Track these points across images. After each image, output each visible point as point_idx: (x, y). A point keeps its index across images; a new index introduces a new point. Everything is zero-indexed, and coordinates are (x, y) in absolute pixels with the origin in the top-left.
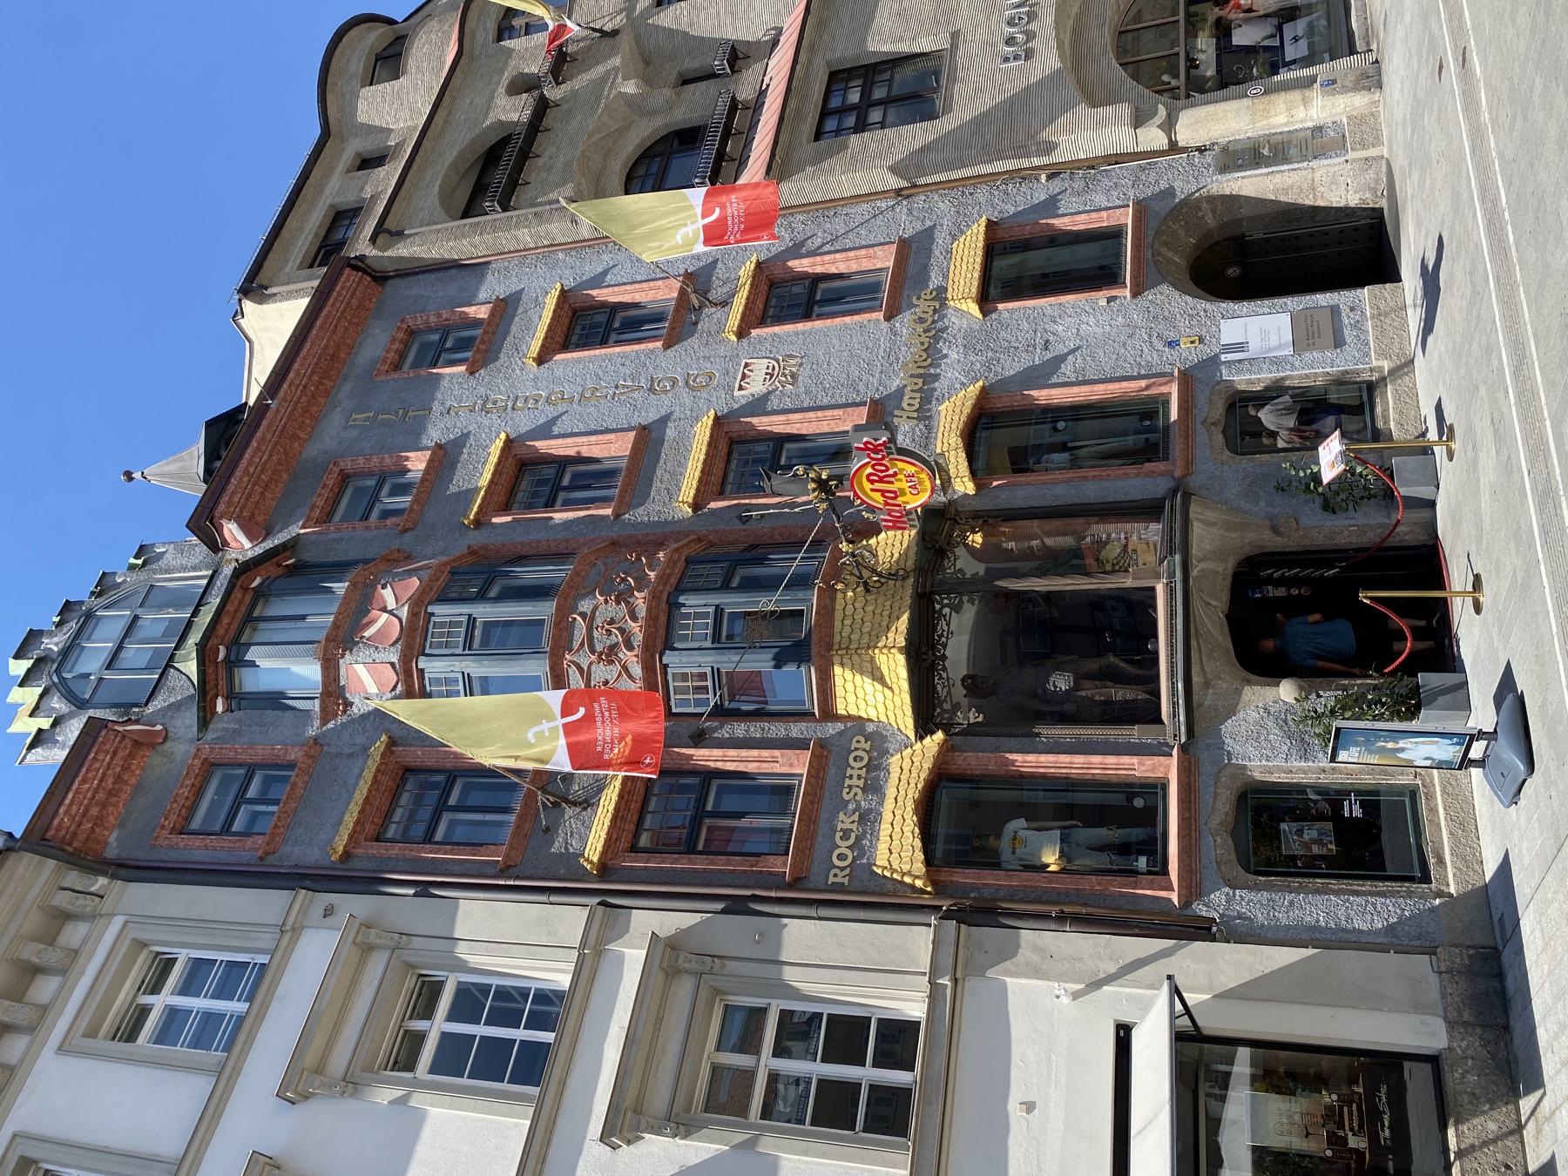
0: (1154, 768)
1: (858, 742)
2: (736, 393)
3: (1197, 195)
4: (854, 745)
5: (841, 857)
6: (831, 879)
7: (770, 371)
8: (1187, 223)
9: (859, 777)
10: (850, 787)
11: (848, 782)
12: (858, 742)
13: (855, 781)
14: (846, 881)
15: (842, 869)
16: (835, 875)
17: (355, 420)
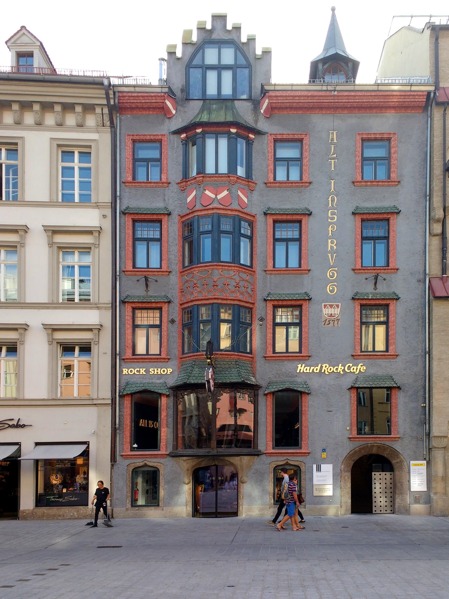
0: (163, 448)
1: (170, 370)
2: (323, 304)
3: (402, 457)
4: (169, 369)
5: (131, 371)
6: (124, 369)
7: (333, 315)
8: (391, 454)
9: (157, 372)
10: (154, 370)
11: (156, 369)
12: (170, 370)
13: (156, 371)
14: (124, 373)
15: (128, 372)
16: (125, 370)
17: (333, 134)
